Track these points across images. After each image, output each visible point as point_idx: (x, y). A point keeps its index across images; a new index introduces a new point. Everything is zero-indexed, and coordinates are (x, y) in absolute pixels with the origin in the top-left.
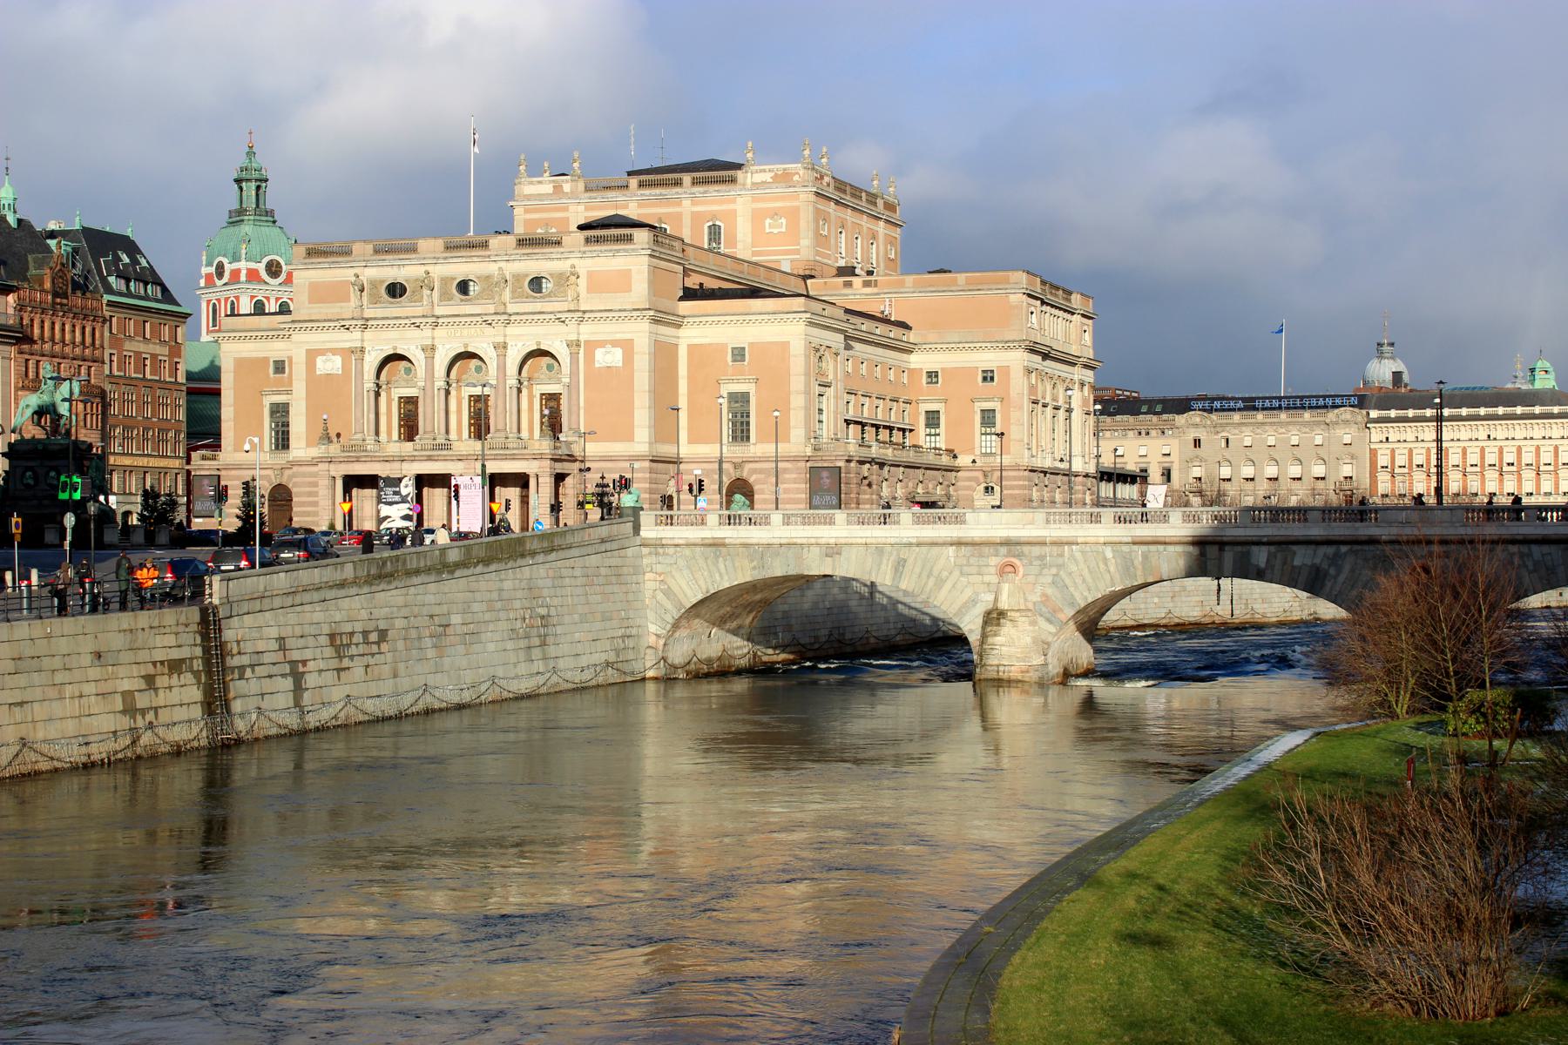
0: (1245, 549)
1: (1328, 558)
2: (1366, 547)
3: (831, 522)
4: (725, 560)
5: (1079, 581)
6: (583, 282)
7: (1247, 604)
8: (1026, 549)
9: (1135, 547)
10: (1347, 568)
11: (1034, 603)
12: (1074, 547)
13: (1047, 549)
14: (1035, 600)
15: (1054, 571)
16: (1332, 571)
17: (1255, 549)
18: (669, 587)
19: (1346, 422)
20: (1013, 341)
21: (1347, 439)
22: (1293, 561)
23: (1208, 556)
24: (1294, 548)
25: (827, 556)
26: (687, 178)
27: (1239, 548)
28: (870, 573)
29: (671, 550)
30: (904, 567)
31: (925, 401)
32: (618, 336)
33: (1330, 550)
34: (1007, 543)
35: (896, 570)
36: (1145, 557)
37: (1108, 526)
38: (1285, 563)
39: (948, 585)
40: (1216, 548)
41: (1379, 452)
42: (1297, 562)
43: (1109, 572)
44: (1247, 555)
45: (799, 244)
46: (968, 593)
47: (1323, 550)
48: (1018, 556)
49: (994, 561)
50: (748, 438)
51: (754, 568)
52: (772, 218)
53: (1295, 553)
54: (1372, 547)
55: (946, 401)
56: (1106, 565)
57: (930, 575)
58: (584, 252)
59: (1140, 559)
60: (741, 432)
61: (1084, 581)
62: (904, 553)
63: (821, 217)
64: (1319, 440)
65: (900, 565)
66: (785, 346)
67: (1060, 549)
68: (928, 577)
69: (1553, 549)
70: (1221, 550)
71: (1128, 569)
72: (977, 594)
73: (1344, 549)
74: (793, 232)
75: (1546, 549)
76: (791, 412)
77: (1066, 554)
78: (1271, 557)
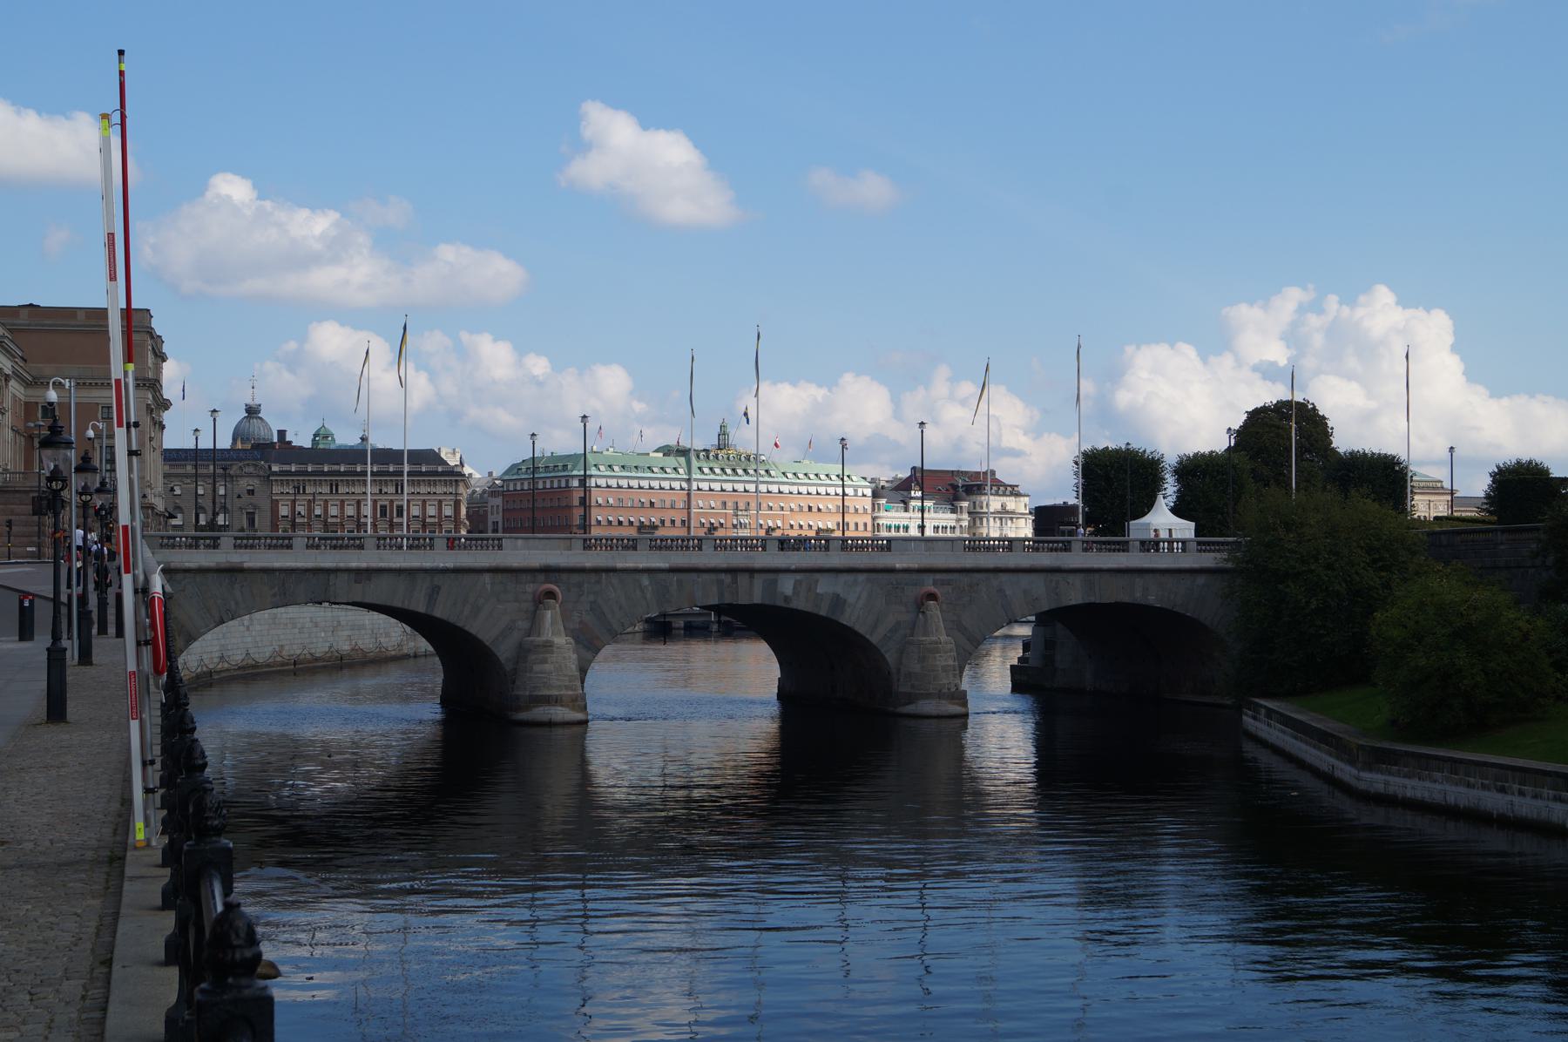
0: (771, 576)
7: (376, 639)
8: (564, 576)
15: (592, 598)
17: (781, 576)
24: (817, 576)
25: (356, 582)
30: (438, 593)
34: (548, 571)
44: (775, 582)
48: (555, 583)
49: (530, 588)
51: (274, 595)
53: (817, 581)
65: (434, 591)
70: (752, 577)
78: (797, 584)
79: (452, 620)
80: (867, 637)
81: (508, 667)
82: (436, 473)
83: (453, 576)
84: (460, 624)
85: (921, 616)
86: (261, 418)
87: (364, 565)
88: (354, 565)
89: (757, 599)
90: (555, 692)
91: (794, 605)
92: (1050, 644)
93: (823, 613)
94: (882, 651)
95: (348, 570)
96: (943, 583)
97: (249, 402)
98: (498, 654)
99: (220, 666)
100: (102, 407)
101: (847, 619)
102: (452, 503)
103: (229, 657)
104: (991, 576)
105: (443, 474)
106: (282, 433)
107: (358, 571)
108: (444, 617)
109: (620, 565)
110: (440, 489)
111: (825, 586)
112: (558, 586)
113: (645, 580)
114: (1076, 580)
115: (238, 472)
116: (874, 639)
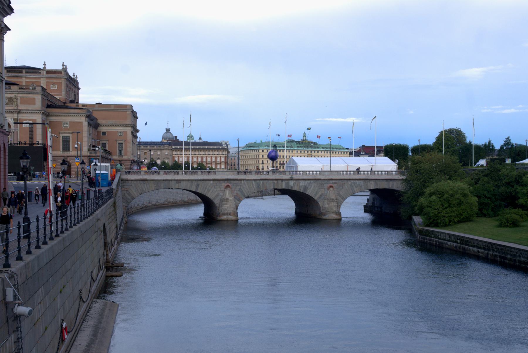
0: (288, 181)
1: (308, 184)
2: (317, 181)
3: (178, 174)
4: (147, 184)
5: (246, 189)
6: (19, 101)
8: (232, 181)
9: (261, 181)
10: (313, 186)
11: (234, 196)
12: (245, 181)
13: (238, 181)
14: (234, 194)
15: (239, 187)
16: (309, 187)
18: (129, 192)
19: (166, 149)
20: (128, 124)
21: (166, 154)
22: (300, 184)
23: (279, 183)
24: (300, 181)
25: (177, 183)
26: (24, 71)
27: (286, 181)
28: (189, 188)
29: (130, 182)
30: (199, 186)
31: (102, 140)
32: (31, 118)
33: (309, 182)
34: (227, 180)
35: (197, 187)
36: (263, 183)
37: (253, 175)
38: (298, 185)
39: (211, 191)
40: (281, 181)
41: (175, 157)
42: (301, 185)
43: (254, 187)
44: (289, 182)
45: (62, 93)
46: (216, 193)
47: (307, 182)
48: (230, 183)
49: (223, 184)
50: (69, 149)
51: (155, 187)
52: (52, 85)
53: (300, 182)
54: (319, 181)
55: (108, 141)
56: (253, 185)
57: (206, 188)
58: (19, 92)
59: (262, 184)
60: (66, 147)
61: (247, 189)
62: (199, 182)
63: (67, 86)
64: (159, 154)
65: (198, 185)
66: (81, 123)
67: (241, 181)
68: (205, 189)
69: (362, 182)
71: (259, 186)
72: (219, 193)
73: (312, 181)
74: (59, 90)
75: (360, 181)
76: (83, 142)
77: (243, 182)
79: (202, 193)
80: (314, 197)
81: (217, 205)
82: (219, 149)
83: (202, 181)
84: (204, 194)
85: (328, 192)
86: (170, 132)
87: (179, 179)
88: (176, 179)
89: (284, 187)
90: (229, 212)
91: (293, 189)
92: (374, 199)
93: (301, 191)
94: (318, 201)
95: (175, 180)
96: (335, 183)
97: (167, 128)
98: (215, 202)
99: (149, 204)
100: (119, 132)
101: (308, 193)
102: (224, 157)
103: (152, 202)
104: (348, 181)
105: (222, 149)
106: (176, 137)
107: (177, 180)
108: (200, 192)
109: (247, 179)
110: (220, 153)
111: (302, 183)
112: (231, 184)
113: (254, 182)
114: (372, 182)
115: (163, 148)
116: (316, 198)
